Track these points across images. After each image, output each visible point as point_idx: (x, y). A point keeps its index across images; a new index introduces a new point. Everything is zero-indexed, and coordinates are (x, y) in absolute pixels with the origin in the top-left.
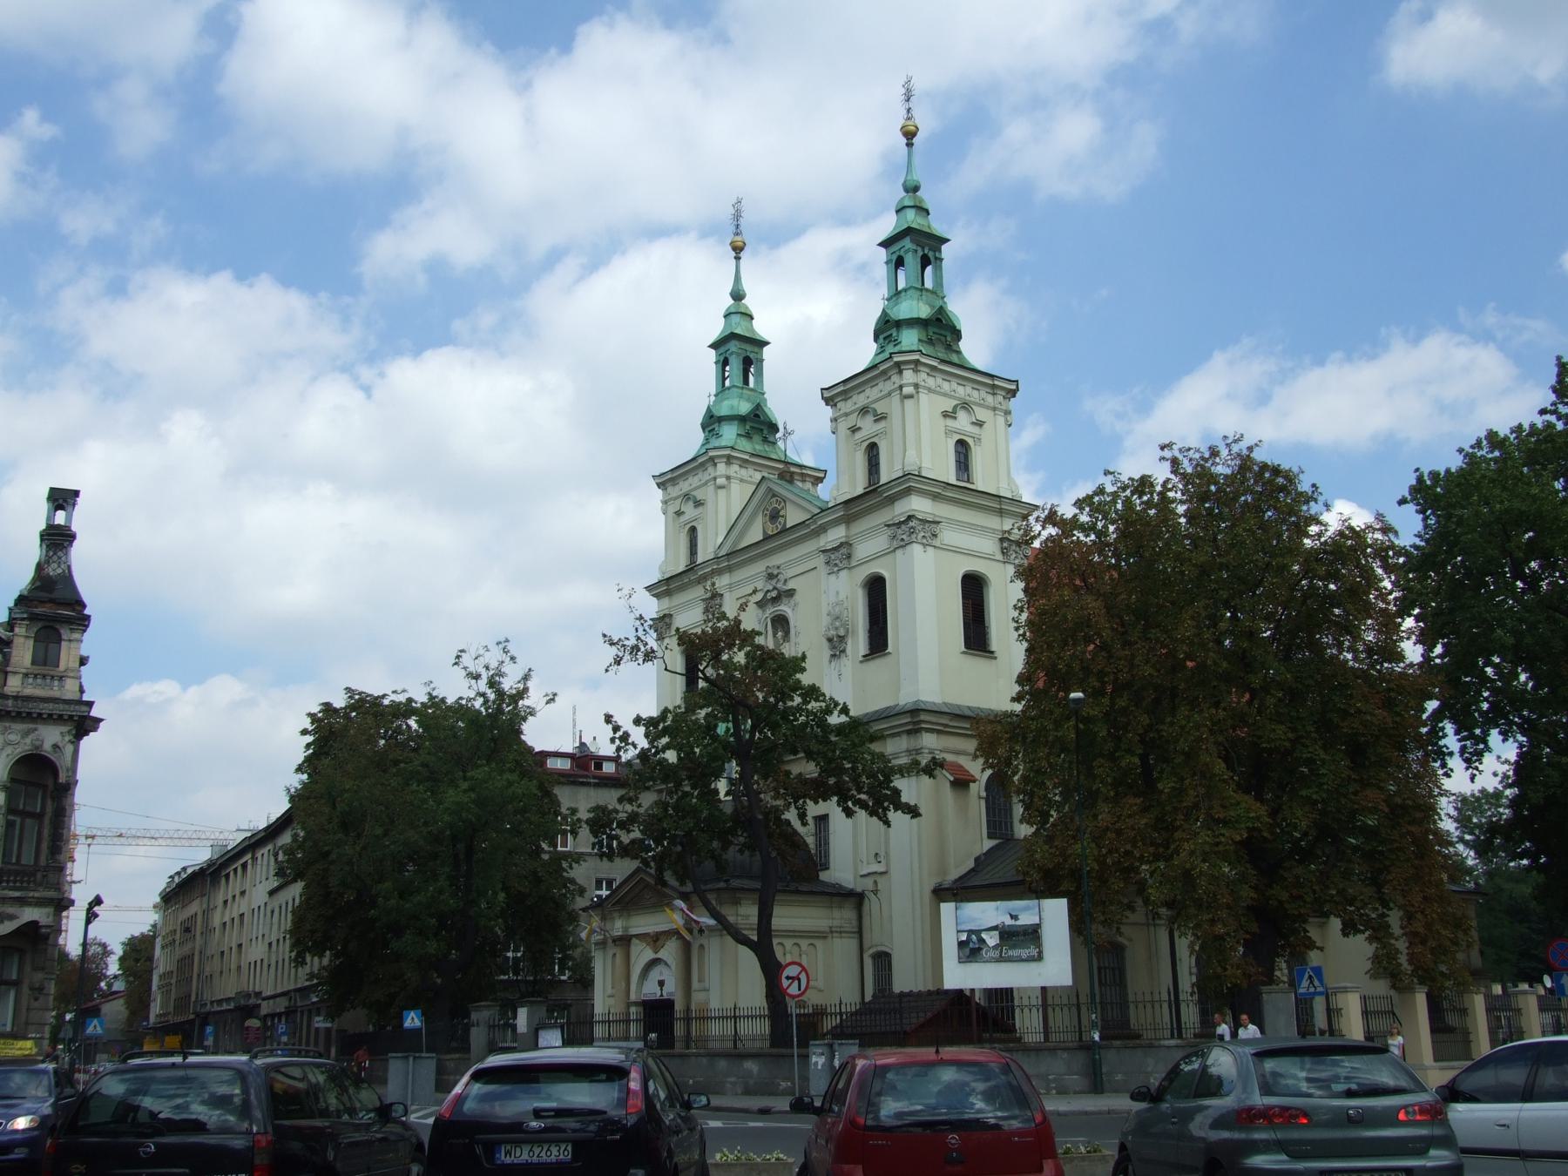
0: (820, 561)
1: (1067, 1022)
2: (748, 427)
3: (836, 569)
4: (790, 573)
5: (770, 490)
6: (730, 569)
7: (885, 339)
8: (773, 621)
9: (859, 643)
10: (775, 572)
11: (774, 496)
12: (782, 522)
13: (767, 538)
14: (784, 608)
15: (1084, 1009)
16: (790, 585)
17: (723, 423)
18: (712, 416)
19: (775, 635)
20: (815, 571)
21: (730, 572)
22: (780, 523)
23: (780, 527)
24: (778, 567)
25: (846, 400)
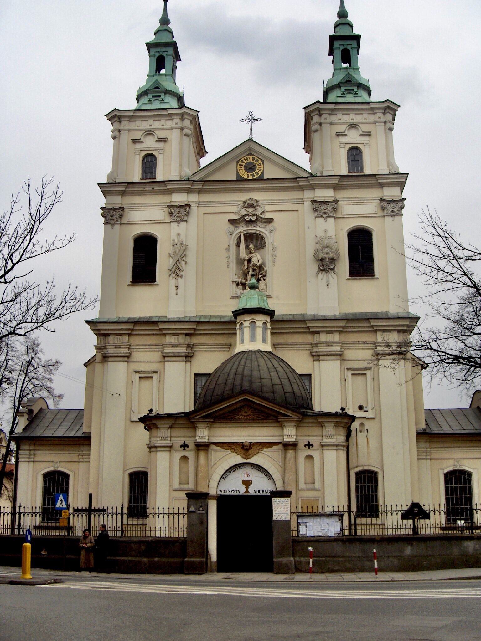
0: (308, 206)
1: (181, 525)
3: (325, 216)
4: (267, 208)
5: (250, 149)
6: (200, 192)
7: (345, 90)
8: (245, 235)
9: (344, 265)
10: (255, 204)
11: (250, 154)
12: (260, 173)
13: (240, 180)
14: (258, 229)
15: (125, 516)
16: (267, 216)
17: (167, 95)
19: (247, 247)
20: (296, 212)
21: (198, 194)
22: (257, 174)
23: (256, 176)
24: (257, 201)
25: (330, 114)
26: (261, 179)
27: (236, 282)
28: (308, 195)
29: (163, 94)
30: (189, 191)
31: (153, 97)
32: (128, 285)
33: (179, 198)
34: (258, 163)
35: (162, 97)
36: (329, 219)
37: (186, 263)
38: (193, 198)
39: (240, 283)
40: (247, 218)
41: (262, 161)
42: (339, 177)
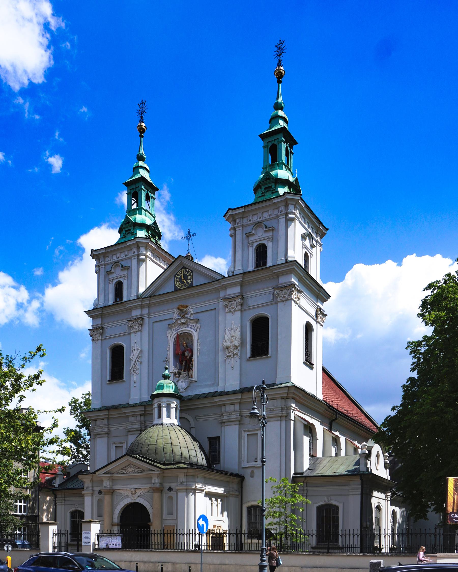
2: (150, 232)
5: (182, 263)
11: (184, 267)
17: (136, 227)
18: (129, 223)
22: (188, 283)
23: (188, 285)
26: (191, 286)
27: (173, 372)
28: (222, 294)
29: (133, 227)
30: (142, 307)
31: (126, 231)
32: (108, 384)
33: (136, 313)
34: (189, 274)
35: (132, 230)
36: (236, 313)
37: (141, 363)
38: (146, 311)
39: (177, 373)
40: (179, 321)
41: (192, 272)
42: (242, 275)
